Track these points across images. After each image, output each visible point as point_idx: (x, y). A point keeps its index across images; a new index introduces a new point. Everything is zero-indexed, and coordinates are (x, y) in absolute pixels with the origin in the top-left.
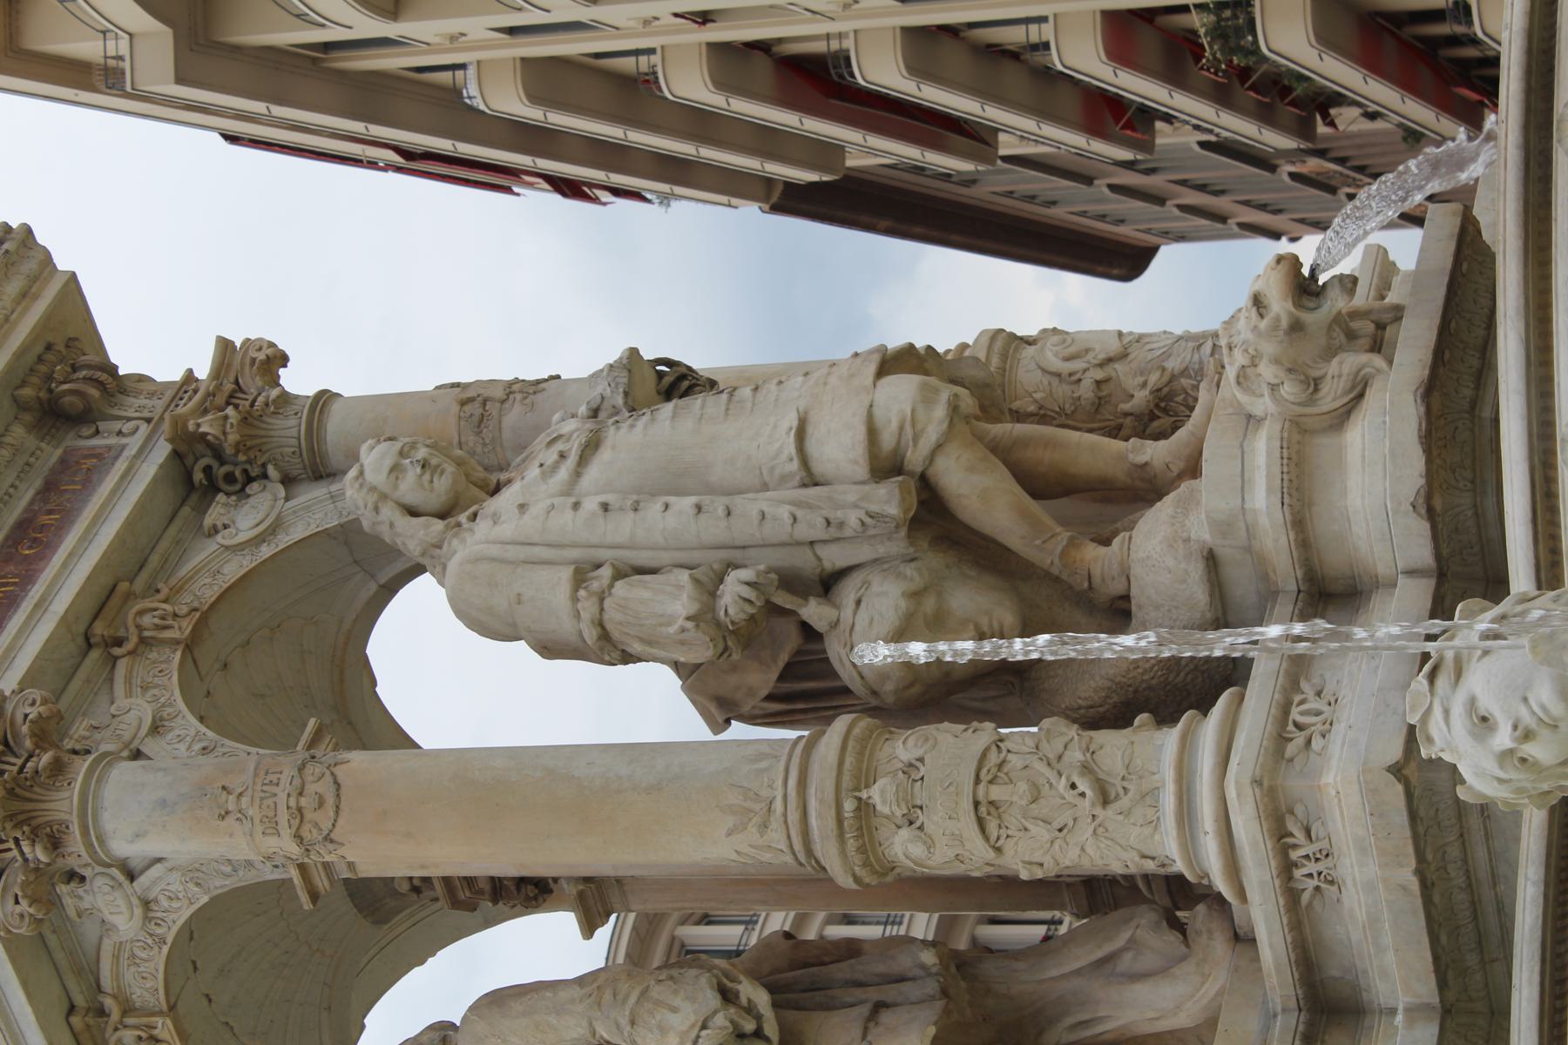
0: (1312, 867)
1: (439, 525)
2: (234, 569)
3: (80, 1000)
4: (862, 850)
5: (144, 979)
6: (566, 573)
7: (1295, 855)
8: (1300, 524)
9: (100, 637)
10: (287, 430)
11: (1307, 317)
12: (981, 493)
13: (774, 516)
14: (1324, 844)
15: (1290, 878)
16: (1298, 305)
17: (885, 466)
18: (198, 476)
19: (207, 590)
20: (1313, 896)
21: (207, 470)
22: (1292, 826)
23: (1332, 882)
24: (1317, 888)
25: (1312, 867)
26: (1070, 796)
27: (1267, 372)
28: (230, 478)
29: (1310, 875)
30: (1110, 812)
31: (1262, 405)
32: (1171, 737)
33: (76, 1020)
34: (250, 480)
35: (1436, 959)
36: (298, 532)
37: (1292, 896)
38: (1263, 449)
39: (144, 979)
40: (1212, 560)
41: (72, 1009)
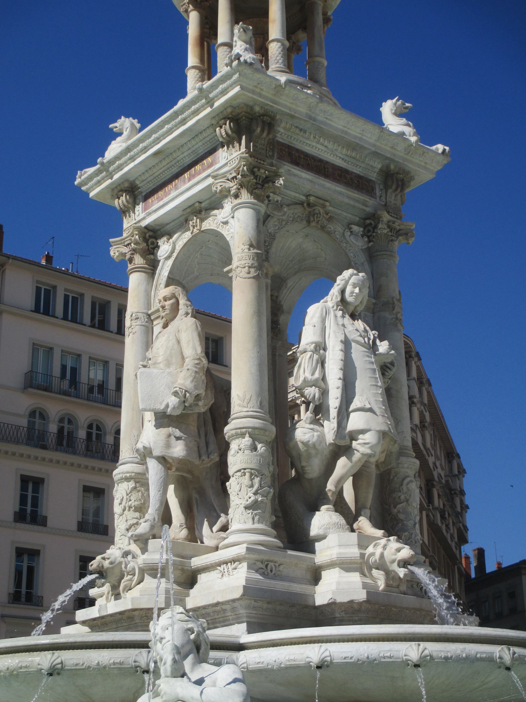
0: (226, 570)
3: (203, 205)
4: (233, 436)
5: (209, 224)
7: (229, 564)
11: (396, 564)
14: (231, 574)
15: (224, 564)
16: (399, 561)
18: (368, 222)
20: (220, 570)
21: (371, 224)
22: (237, 563)
23: (222, 576)
24: (221, 571)
25: (226, 570)
26: (247, 497)
28: (369, 231)
29: (224, 569)
30: (243, 509)
33: (197, 204)
34: (368, 237)
35: (199, 608)
37: (219, 564)
39: (209, 224)
41: (200, 203)
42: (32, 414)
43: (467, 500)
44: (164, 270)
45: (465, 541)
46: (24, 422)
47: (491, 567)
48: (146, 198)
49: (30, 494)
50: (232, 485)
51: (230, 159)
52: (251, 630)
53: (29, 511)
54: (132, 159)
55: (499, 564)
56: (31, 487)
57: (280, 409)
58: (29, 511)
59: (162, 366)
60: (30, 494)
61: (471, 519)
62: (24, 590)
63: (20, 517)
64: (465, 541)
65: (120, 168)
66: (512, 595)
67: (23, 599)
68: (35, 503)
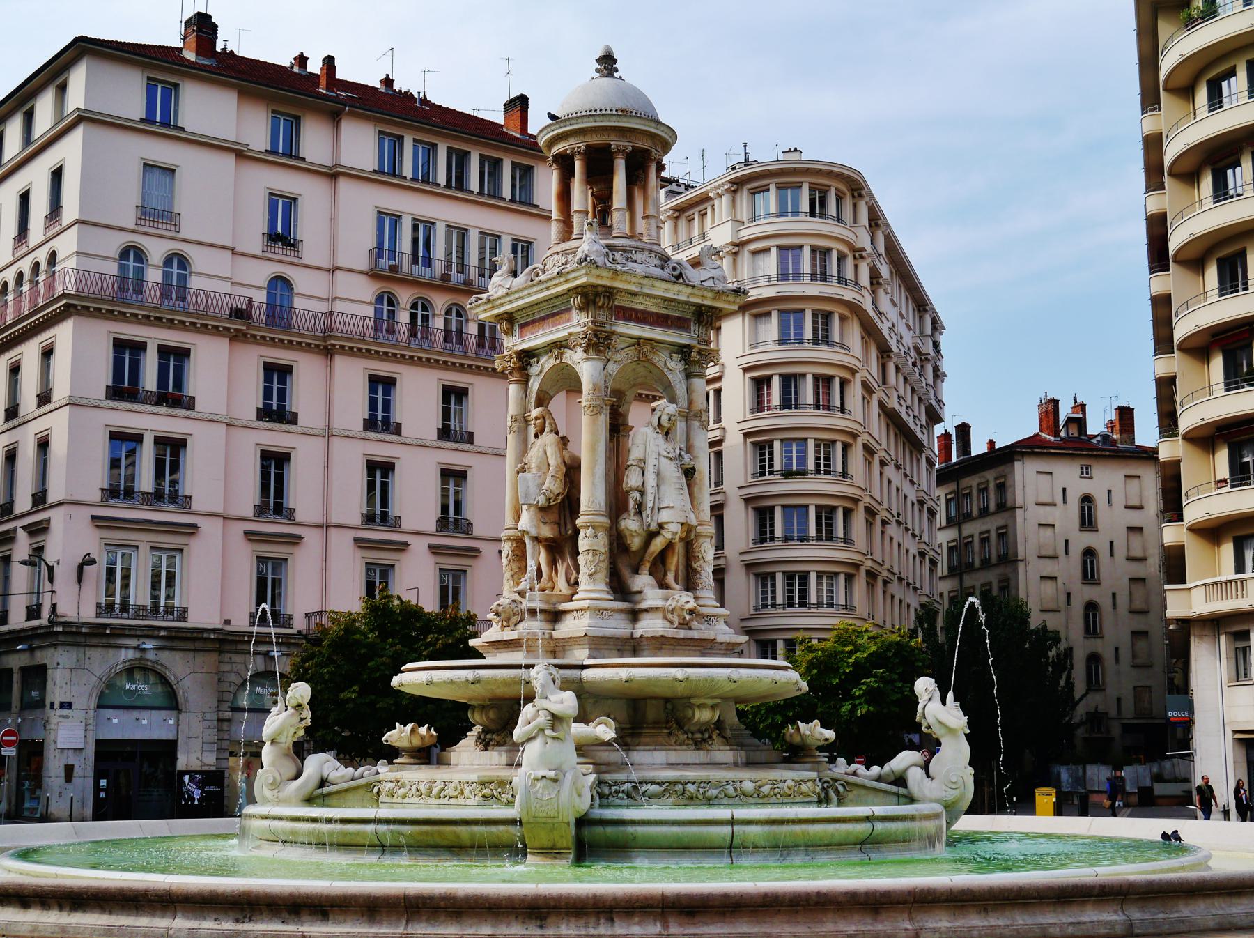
1: (656, 424)
2: (660, 364)
6: (641, 457)
8: (646, 610)
9: (639, 342)
10: (696, 369)
12: (658, 544)
13: (649, 501)
17: (661, 526)
19: (655, 359)
27: (674, 604)
31: (670, 602)
32: (603, 587)
36: (670, 377)
38: (660, 603)
40: (640, 592)
42: (379, 299)
43: (945, 366)
44: (535, 384)
45: (939, 420)
46: (369, 311)
47: (978, 447)
48: (522, 326)
49: (380, 397)
50: (581, 559)
51: (578, 323)
52: (590, 657)
53: (380, 418)
54: (511, 302)
55: (992, 443)
56: (381, 386)
57: (618, 502)
58: (380, 418)
59: (534, 471)
60: (380, 397)
61: (948, 390)
62: (378, 510)
63: (370, 424)
64: (939, 420)
65: (501, 305)
66: (1001, 487)
67: (378, 520)
68: (387, 406)
